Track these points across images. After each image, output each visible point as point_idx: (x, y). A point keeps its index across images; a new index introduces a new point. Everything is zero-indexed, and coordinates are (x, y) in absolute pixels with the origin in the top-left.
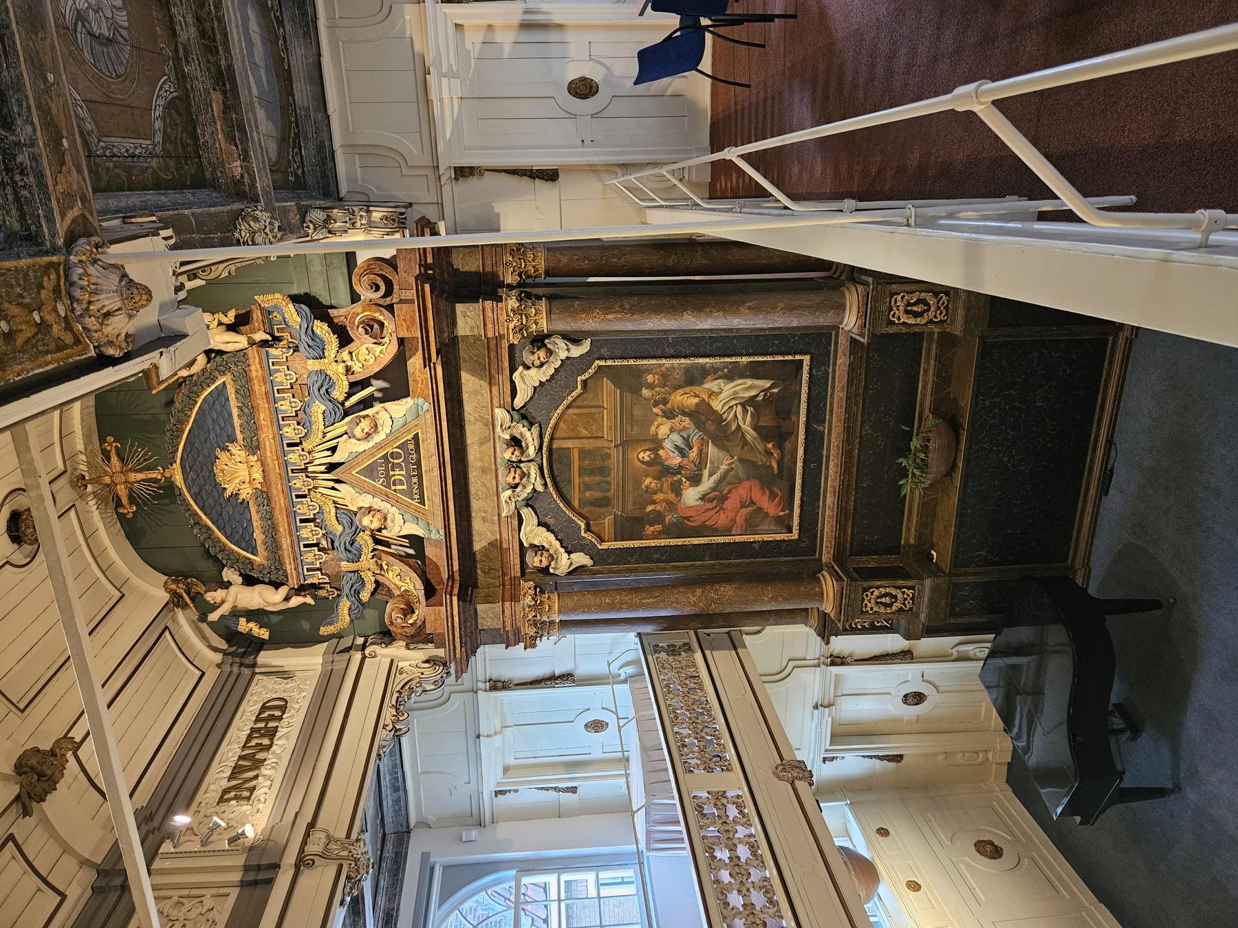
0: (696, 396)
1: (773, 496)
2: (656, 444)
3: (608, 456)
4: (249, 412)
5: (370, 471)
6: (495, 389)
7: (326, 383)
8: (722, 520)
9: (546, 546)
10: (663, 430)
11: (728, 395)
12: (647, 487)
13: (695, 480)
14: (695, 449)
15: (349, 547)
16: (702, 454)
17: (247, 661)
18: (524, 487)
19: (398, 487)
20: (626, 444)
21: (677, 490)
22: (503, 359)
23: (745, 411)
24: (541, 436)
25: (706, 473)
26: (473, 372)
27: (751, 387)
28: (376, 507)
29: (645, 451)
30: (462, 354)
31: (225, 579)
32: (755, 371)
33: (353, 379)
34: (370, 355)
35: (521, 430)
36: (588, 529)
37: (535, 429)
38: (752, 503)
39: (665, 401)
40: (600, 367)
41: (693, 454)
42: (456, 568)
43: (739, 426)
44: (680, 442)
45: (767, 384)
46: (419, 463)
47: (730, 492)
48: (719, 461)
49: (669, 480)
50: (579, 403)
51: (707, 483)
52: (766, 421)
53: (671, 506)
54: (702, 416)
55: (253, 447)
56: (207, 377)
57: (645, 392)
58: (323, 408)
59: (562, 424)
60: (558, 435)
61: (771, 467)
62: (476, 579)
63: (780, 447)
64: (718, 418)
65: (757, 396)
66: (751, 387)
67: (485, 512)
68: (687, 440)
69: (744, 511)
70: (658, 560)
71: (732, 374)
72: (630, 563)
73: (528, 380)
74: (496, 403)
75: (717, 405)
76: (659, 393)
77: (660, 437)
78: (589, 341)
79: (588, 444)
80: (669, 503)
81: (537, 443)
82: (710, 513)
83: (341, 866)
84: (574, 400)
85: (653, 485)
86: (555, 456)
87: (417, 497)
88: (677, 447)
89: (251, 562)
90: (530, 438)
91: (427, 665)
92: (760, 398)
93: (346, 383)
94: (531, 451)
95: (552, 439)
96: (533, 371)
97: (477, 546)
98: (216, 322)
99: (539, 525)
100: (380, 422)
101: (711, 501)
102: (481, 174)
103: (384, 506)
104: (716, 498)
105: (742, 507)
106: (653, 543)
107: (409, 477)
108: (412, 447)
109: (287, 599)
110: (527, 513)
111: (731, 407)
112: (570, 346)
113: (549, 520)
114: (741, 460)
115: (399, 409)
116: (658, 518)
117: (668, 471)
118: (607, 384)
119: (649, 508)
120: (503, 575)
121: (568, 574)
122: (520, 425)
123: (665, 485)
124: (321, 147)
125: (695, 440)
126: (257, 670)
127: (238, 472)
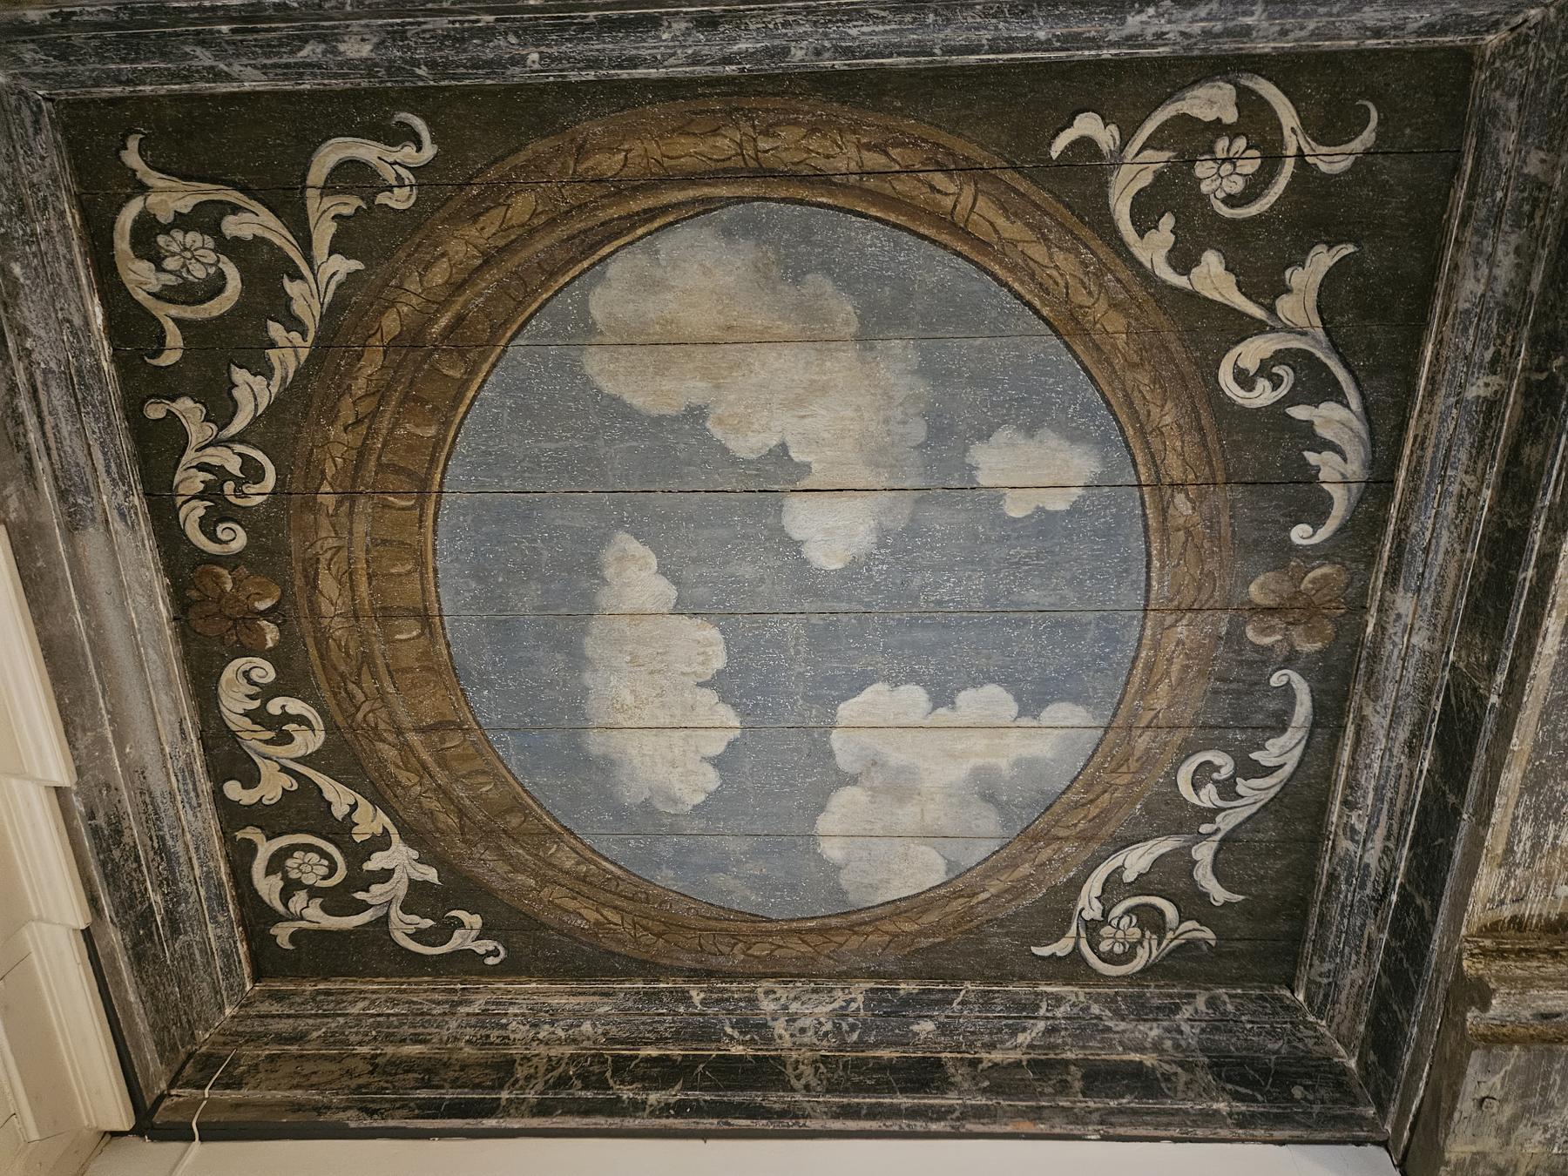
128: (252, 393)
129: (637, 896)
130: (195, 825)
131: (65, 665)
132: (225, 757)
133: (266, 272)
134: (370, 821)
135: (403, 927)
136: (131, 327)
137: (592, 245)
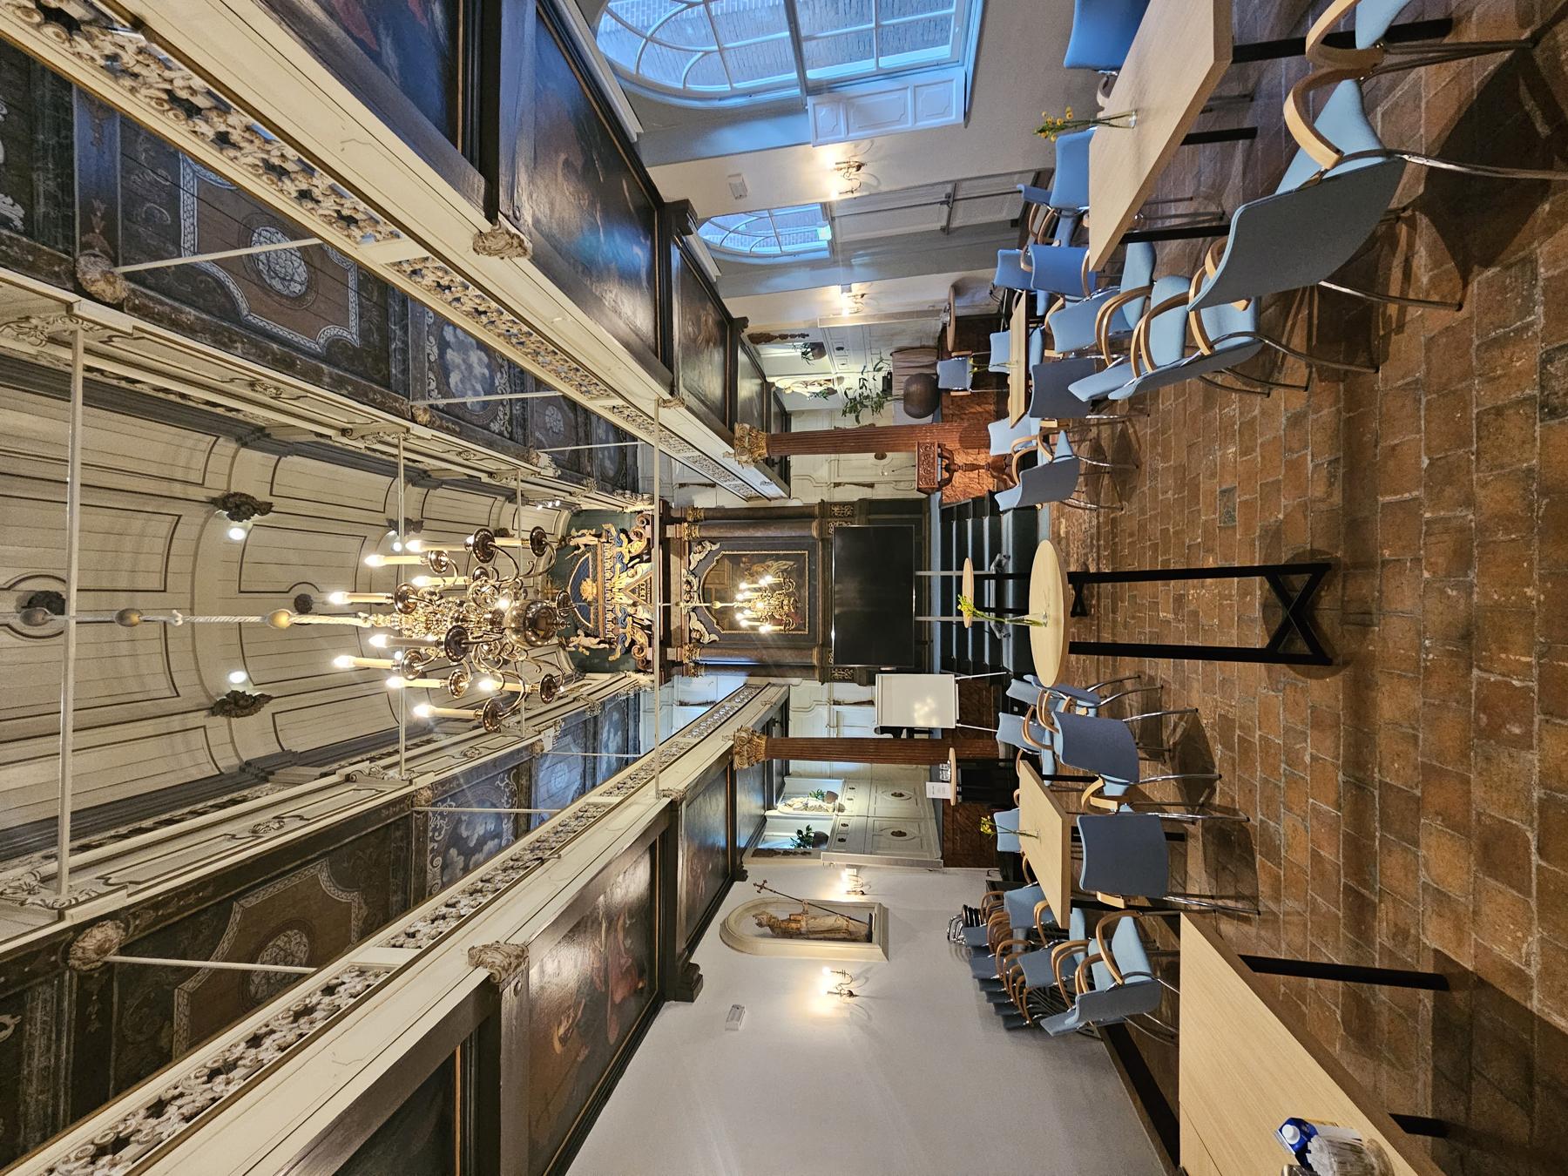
4: (595, 568)
5: (633, 591)
7: (621, 556)
22: (685, 548)
32: (786, 557)
34: (638, 546)
35: (691, 578)
55: (595, 580)
56: (584, 553)
73: (696, 558)
90: (695, 582)
115: (645, 566)
127: (588, 589)
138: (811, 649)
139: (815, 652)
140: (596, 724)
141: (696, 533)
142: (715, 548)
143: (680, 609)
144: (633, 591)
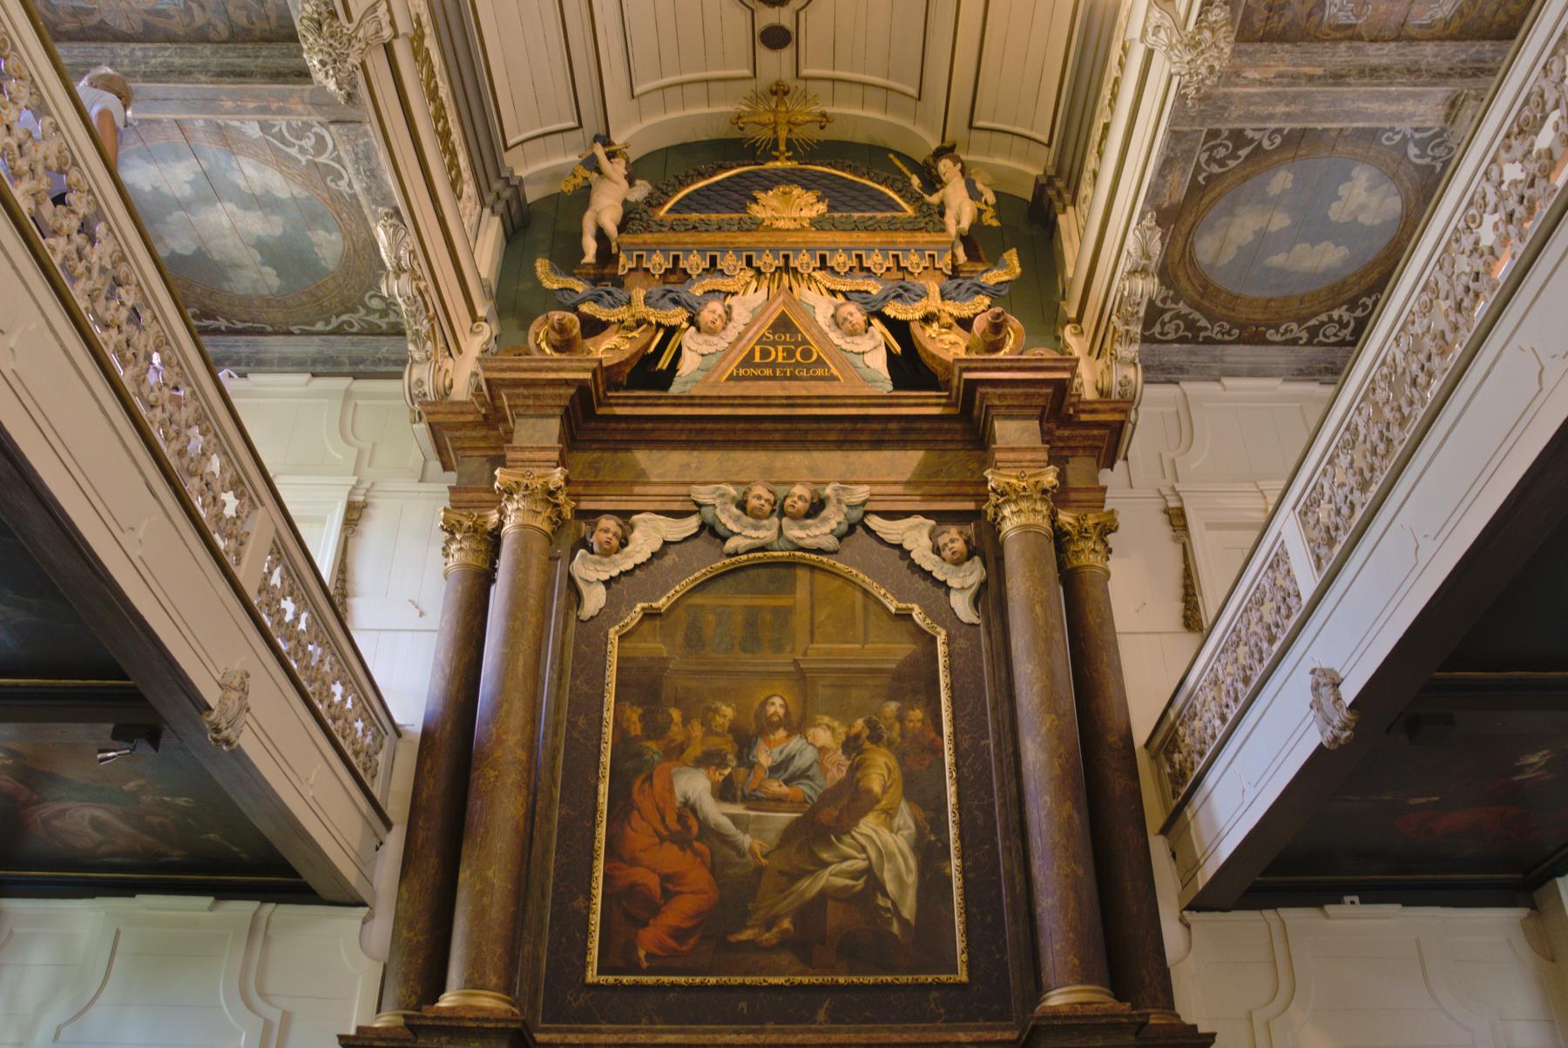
0: (885, 789)
1: (680, 934)
2: (797, 725)
3: (779, 649)
6: (898, 489)
8: (639, 835)
9: (627, 549)
10: (823, 736)
11: (885, 840)
12: (716, 711)
13: (724, 792)
14: (785, 789)
15: (671, 295)
16: (778, 802)
17: (500, 206)
18: (737, 520)
19: (757, 355)
20: (801, 678)
21: (708, 760)
23: (855, 875)
24: (820, 551)
25: (738, 809)
26: (923, 465)
27: (901, 882)
28: (730, 325)
29: (785, 706)
30: (949, 456)
31: (638, 182)
32: (932, 884)
33: (916, 329)
35: (833, 518)
36: (650, 615)
37: (830, 542)
38: (668, 895)
39: (876, 737)
40: (933, 639)
41: (776, 787)
42: (619, 411)
43: (826, 865)
44: (800, 763)
45: (908, 910)
46: (793, 378)
47: (696, 853)
48: (756, 835)
49: (728, 746)
50: (873, 608)
51: (717, 813)
52: (835, 917)
53: (676, 752)
54: (851, 800)
55: (818, 224)
56: (914, 199)
57: (892, 707)
58: (874, 292)
59: (838, 583)
60: (819, 577)
61: (743, 927)
62: (585, 450)
63: (784, 943)
64: (844, 826)
65: (886, 895)
66: (901, 882)
67: (698, 468)
68: (803, 775)
69: (653, 882)
70: (572, 725)
71: (929, 853)
72: (574, 677)
74: (879, 489)
75: (869, 826)
76: (890, 728)
77: (811, 731)
78: (976, 620)
79: (801, 621)
80: (681, 749)
81: (808, 542)
82: (655, 818)
83: (350, 19)
84: (878, 602)
85: (720, 720)
86: (783, 572)
87: (742, 372)
88: (790, 759)
89: (661, 205)
90: (819, 533)
91: (447, 382)
92: (881, 901)
93: (910, 317)
94: (794, 532)
95: (812, 568)
96: (926, 542)
97: (642, 457)
98: (983, 207)
99: (666, 544)
100: (857, 339)
101: (681, 818)
102: (1176, 539)
103: (732, 333)
104: (687, 826)
105: (666, 878)
106: (609, 715)
107: (774, 365)
108: (819, 372)
109: (601, 235)
110: (692, 524)
111: (863, 849)
112: (969, 593)
113: (671, 558)
114: (759, 871)
116: (655, 728)
117: (745, 741)
118: (903, 649)
119: (676, 714)
120: (587, 484)
121: (571, 579)
122: (841, 518)
123: (718, 740)
124: (1181, 369)
125: (804, 789)
126: (487, 211)
128: (1203, 322)
129: (1373, 265)
130: (1308, 350)
131: (1254, 372)
132: (1294, 342)
133: (1178, 316)
134: (1324, 317)
135: (1359, 313)
136: (1182, 340)
137: (1192, 262)
138: (508, 989)
139: (489, 1001)
140: (277, 76)
141: (1012, 522)
142: (961, 604)
143: (714, 479)
144: (783, 324)
